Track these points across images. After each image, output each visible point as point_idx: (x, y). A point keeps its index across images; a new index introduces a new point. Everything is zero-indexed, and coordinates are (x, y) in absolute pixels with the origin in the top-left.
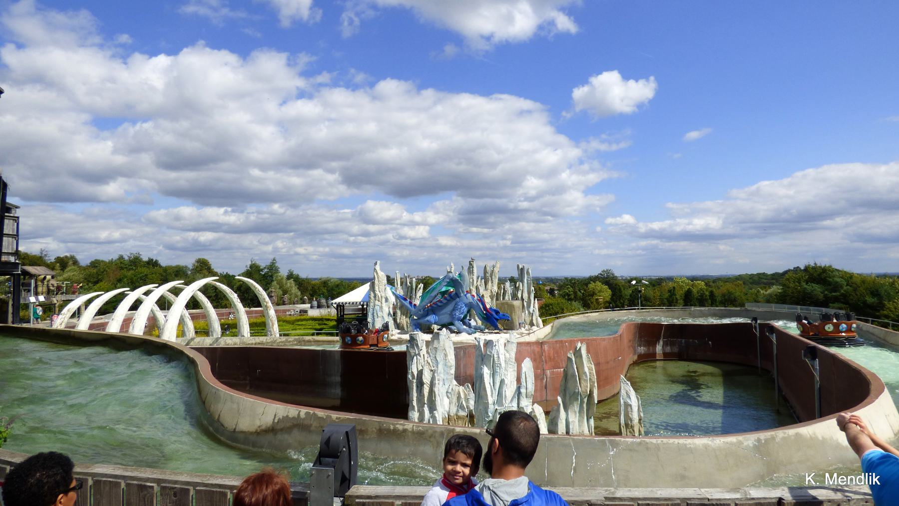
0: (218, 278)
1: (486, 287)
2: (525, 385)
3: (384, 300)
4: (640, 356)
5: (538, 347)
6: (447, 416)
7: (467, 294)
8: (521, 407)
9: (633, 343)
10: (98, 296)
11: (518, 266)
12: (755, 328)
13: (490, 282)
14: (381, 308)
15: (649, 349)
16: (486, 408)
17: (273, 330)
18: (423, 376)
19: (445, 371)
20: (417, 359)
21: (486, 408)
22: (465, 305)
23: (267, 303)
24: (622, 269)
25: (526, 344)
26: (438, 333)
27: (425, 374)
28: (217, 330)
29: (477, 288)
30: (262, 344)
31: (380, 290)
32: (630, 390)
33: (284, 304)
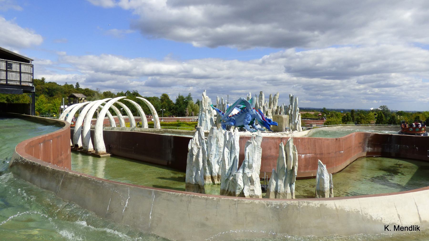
0: (126, 97)
1: (270, 107)
2: (248, 160)
3: (207, 111)
4: (368, 153)
6: (217, 175)
7: (253, 109)
8: (245, 173)
9: (362, 145)
10: (85, 106)
11: (290, 95)
13: (272, 104)
14: (206, 115)
16: (224, 171)
17: (157, 125)
18: (193, 151)
19: (217, 150)
20: (191, 141)
21: (224, 171)
22: (251, 116)
23: (153, 111)
24: (393, 108)
25: (271, 138)
26: (213, 128)
27: (195, 150)
28: (134, 124)
29: (264, 107)
30: (149, 132)
31: (205, 106)
32: (324, 170)
33: (192, 116)
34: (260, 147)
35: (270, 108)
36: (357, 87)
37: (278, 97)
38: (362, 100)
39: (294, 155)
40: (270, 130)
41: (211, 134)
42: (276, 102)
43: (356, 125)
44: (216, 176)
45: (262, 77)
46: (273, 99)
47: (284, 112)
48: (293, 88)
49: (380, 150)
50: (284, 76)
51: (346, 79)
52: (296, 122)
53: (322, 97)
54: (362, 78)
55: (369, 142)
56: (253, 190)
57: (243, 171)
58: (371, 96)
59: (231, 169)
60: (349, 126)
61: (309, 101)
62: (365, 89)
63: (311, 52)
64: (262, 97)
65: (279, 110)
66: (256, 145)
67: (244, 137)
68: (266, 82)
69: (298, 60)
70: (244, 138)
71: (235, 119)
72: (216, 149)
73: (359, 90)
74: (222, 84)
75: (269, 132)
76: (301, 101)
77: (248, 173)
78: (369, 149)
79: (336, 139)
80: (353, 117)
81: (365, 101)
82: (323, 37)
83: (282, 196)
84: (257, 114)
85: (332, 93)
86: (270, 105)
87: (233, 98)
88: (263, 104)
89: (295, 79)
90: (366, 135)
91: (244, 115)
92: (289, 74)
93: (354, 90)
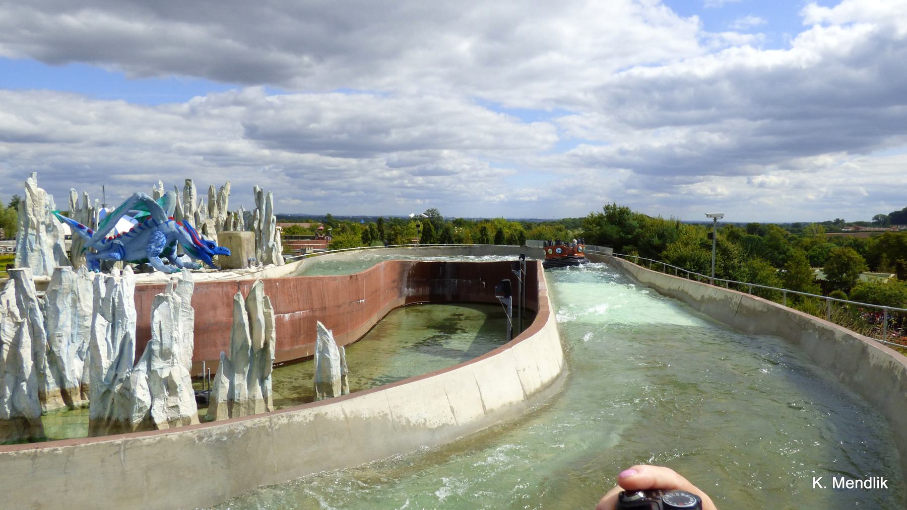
1: (210, 214)
2: (159, 340)
5: (233, 288)
6: (78, 385)
7: (169, 221)
9: (398, 285)
11: (255, 189)
12: (523, 265)
15: (418, 290)
22: (166, 236)
24: (449, 212)
25: (215, 285)
26: (60, 269)
29: (196, 215)
32: (328, 340)
34: (189, 306)
35: (211, 217)
36: (387, 174)
37: (228, 193)
38: (397, 199)
39: (267, 316)
40: (214, 265)
41: (54, 286)
42: (224, 202)
43: (386, 247)
44: (75, 387)
45: (192, 146)
46: (218, 196)
47: (244, 224)
48: (264, 172)
49: (426, 291)
50: (243, 146)
51: (366, 157)
52: (270, 245)
53: (323, 192)
54: (395, 156)
55: (408, 277)
56: (177, 406)
57: (149, 366)
58: (411, 190)
59: (117, 365)
60: (374, 250)
61: (297, 201)
62: (401, 177)
63: (297, 97)
64: (190, 192)
65: (233, 220)
66: (180, 301)
67: (147, 286)
68: (201, 158)
69: (271, 112)
70: (149, 287)
71: (122, 244)
72: (73, 322)
73: (391, 179)
74: (85, 159)
75: (210, 270)
76: (283, 201)
77: (162, 369)
78: (410, 291)
79: (351, 277)
80: (382, 231)
81: (402, 201)
82: (320, 70)
83: (245, 408)
84: (180, 231)
85: (343, 184)
86: (210, 210)
87: (120, 192)
88: (194, 208)
89: (266, 152)
90: (403, 264)
91: (147, 234)
92: (252, 141)
93: (383, 179)
